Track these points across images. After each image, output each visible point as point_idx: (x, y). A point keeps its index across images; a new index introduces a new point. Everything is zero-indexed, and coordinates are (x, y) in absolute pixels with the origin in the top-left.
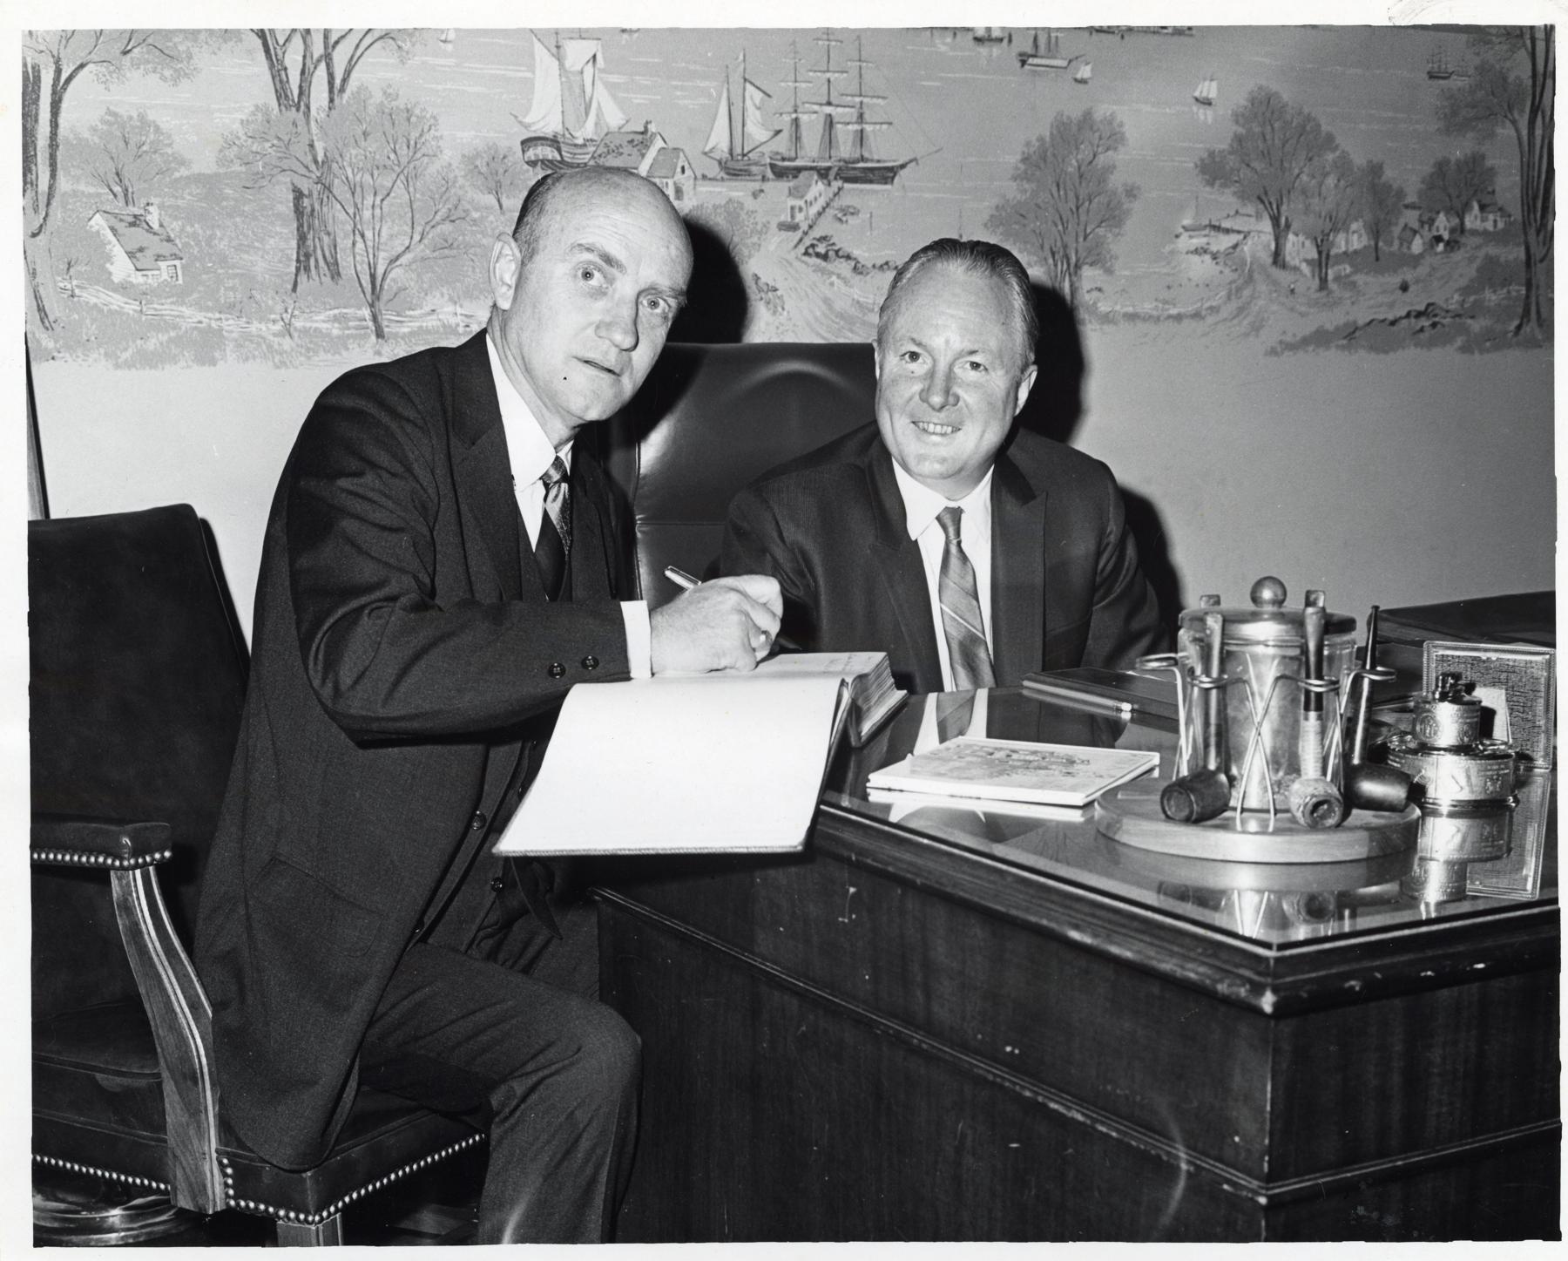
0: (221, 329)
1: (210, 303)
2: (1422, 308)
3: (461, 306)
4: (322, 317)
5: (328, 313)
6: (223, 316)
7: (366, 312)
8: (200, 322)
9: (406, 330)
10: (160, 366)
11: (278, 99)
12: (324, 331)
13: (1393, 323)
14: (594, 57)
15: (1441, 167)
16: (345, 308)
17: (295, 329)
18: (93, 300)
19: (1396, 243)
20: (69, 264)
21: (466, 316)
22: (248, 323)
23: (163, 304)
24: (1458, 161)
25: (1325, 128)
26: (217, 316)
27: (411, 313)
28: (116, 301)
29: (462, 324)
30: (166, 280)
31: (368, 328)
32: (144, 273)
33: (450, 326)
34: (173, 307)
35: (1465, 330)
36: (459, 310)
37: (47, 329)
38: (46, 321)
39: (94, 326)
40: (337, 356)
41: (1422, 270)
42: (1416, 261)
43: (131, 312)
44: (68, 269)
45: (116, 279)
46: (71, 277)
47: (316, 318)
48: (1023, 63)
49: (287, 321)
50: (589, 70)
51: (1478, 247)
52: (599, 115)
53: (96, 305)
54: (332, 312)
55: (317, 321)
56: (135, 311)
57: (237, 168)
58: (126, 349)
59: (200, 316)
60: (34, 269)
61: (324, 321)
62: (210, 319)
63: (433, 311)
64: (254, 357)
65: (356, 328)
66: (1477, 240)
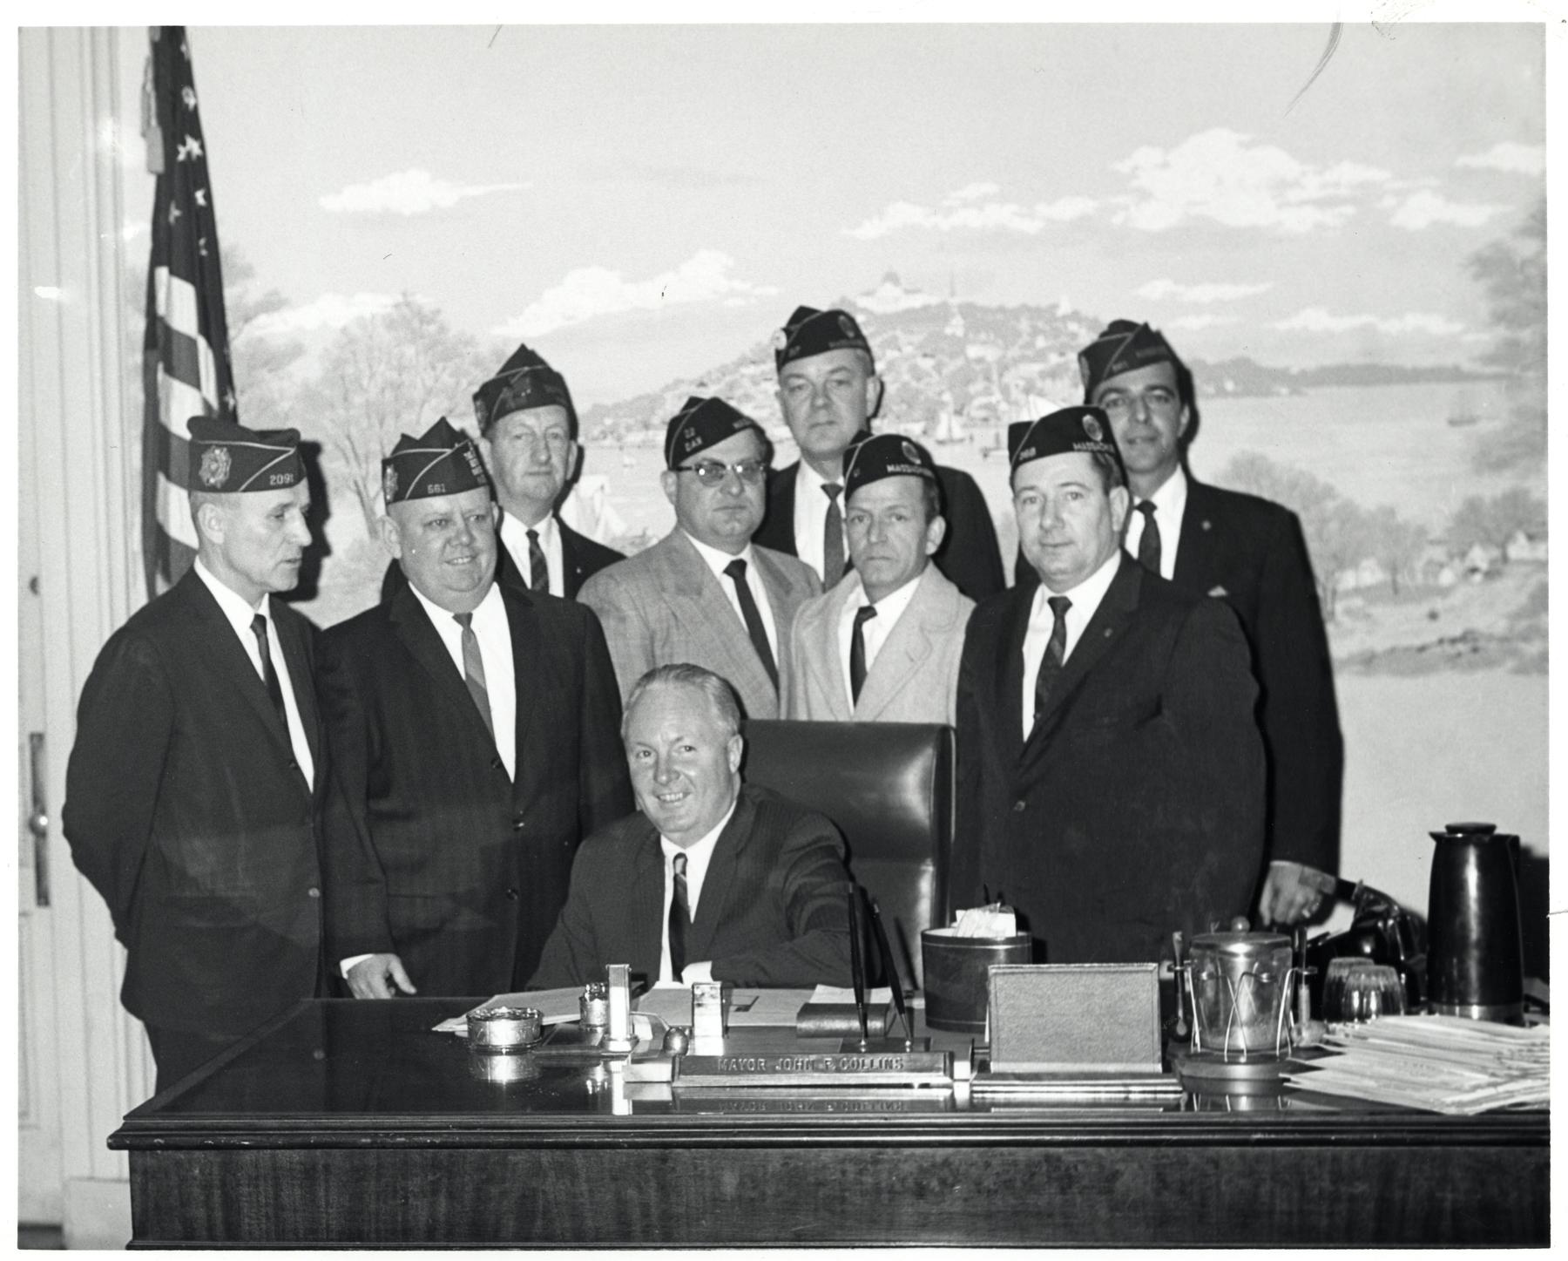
2: (1457, 631)
11: (370, 533)
13: (1422, 649)
14: (602, 488)
15: (1473, 506)
19: (1420, 578)
24: (1495, 503)
25: (1323, 478)
35: (1514, 653)
41: (1456, 599)
42: (1444, 592)
48: (985, 456)
50: (598, 497)
51: (1527, 576)
52: (607, 524)
57: (342, 580)
66: (1524, 569)
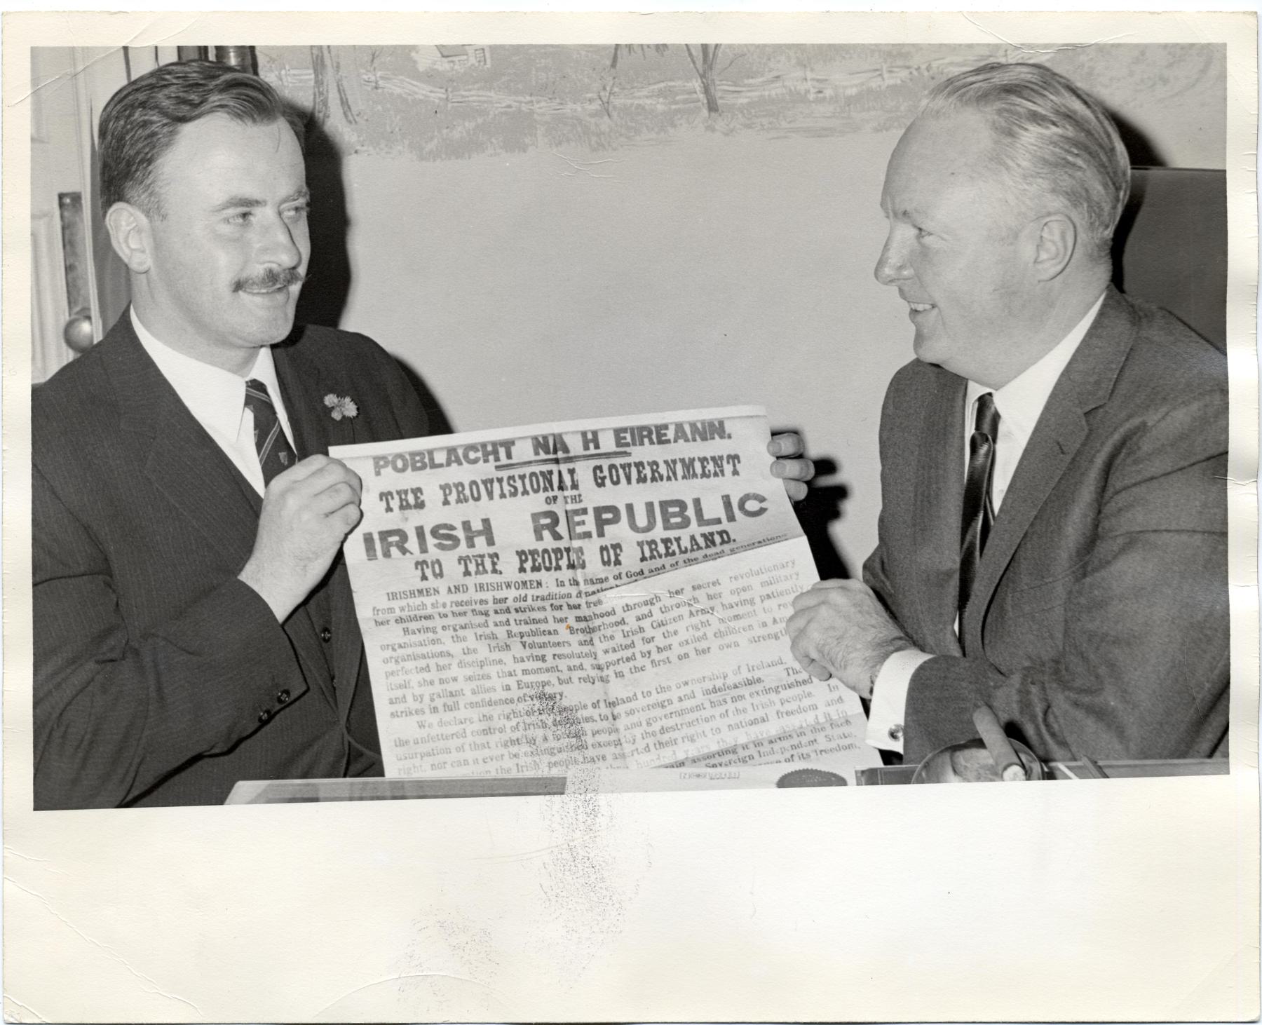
0: (532, 112)
1: (520, 86)
3: (812, 70)
4: (644, 92)
5: (651, 87)
6: (534, 99)
7: (697, 84)
8: (509, 106)
9: (746, 101)
10: (467, 156)
12: (647, 107)
16: (671, 80)
17: (614, 107)
18: (398, 91)
20: (373, 55)
21: (818, 80)
22: (562, 104)
23: (470, 90)
26: (528, 98)
27: (751, 81)
28: (423, 90)
29: (813, 90)
30: (473, 65)
31: (699, 101)
32: (450, 59)
33: (799, 93)
34: (481, 93)
36: (809, 75)
37: (350, 122)
38: (349, 114)
39: (398, 117)
40: (662, 134)
43: (437, 101)
44: (372, 61)
45: (421, 67)
46: (375, 69)
47: (637, 94)
49: (605, 100)
53: (400, 96)
54: (656, 87)
55: (639, 98)
56: (440, 99)
58: (432, 138)
59: (509, 100)
60: (338, 63)
61: (647, 97)
62: (520, 102)
63: (778, 77)
64: (568, 141)
65: (685, 102)
